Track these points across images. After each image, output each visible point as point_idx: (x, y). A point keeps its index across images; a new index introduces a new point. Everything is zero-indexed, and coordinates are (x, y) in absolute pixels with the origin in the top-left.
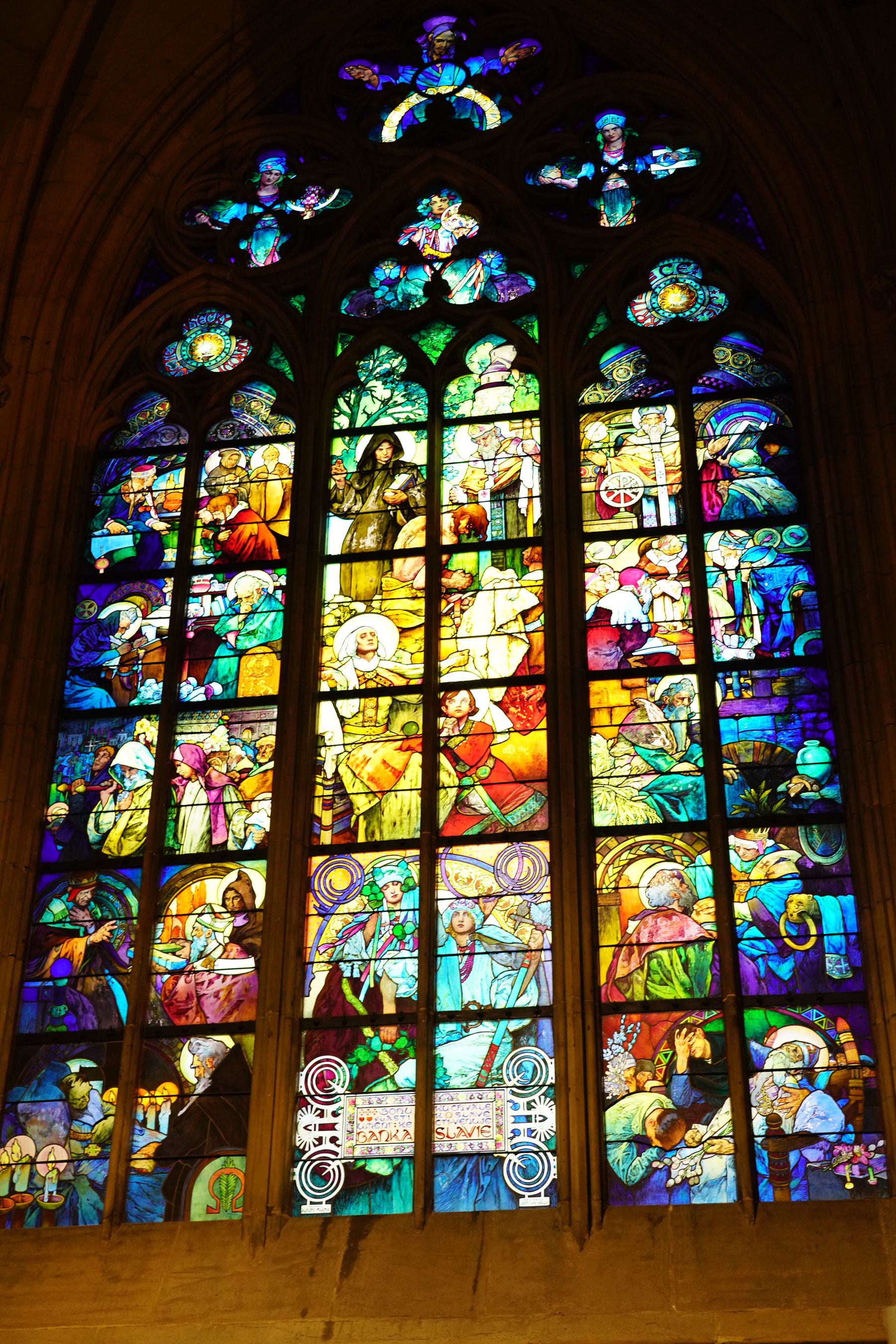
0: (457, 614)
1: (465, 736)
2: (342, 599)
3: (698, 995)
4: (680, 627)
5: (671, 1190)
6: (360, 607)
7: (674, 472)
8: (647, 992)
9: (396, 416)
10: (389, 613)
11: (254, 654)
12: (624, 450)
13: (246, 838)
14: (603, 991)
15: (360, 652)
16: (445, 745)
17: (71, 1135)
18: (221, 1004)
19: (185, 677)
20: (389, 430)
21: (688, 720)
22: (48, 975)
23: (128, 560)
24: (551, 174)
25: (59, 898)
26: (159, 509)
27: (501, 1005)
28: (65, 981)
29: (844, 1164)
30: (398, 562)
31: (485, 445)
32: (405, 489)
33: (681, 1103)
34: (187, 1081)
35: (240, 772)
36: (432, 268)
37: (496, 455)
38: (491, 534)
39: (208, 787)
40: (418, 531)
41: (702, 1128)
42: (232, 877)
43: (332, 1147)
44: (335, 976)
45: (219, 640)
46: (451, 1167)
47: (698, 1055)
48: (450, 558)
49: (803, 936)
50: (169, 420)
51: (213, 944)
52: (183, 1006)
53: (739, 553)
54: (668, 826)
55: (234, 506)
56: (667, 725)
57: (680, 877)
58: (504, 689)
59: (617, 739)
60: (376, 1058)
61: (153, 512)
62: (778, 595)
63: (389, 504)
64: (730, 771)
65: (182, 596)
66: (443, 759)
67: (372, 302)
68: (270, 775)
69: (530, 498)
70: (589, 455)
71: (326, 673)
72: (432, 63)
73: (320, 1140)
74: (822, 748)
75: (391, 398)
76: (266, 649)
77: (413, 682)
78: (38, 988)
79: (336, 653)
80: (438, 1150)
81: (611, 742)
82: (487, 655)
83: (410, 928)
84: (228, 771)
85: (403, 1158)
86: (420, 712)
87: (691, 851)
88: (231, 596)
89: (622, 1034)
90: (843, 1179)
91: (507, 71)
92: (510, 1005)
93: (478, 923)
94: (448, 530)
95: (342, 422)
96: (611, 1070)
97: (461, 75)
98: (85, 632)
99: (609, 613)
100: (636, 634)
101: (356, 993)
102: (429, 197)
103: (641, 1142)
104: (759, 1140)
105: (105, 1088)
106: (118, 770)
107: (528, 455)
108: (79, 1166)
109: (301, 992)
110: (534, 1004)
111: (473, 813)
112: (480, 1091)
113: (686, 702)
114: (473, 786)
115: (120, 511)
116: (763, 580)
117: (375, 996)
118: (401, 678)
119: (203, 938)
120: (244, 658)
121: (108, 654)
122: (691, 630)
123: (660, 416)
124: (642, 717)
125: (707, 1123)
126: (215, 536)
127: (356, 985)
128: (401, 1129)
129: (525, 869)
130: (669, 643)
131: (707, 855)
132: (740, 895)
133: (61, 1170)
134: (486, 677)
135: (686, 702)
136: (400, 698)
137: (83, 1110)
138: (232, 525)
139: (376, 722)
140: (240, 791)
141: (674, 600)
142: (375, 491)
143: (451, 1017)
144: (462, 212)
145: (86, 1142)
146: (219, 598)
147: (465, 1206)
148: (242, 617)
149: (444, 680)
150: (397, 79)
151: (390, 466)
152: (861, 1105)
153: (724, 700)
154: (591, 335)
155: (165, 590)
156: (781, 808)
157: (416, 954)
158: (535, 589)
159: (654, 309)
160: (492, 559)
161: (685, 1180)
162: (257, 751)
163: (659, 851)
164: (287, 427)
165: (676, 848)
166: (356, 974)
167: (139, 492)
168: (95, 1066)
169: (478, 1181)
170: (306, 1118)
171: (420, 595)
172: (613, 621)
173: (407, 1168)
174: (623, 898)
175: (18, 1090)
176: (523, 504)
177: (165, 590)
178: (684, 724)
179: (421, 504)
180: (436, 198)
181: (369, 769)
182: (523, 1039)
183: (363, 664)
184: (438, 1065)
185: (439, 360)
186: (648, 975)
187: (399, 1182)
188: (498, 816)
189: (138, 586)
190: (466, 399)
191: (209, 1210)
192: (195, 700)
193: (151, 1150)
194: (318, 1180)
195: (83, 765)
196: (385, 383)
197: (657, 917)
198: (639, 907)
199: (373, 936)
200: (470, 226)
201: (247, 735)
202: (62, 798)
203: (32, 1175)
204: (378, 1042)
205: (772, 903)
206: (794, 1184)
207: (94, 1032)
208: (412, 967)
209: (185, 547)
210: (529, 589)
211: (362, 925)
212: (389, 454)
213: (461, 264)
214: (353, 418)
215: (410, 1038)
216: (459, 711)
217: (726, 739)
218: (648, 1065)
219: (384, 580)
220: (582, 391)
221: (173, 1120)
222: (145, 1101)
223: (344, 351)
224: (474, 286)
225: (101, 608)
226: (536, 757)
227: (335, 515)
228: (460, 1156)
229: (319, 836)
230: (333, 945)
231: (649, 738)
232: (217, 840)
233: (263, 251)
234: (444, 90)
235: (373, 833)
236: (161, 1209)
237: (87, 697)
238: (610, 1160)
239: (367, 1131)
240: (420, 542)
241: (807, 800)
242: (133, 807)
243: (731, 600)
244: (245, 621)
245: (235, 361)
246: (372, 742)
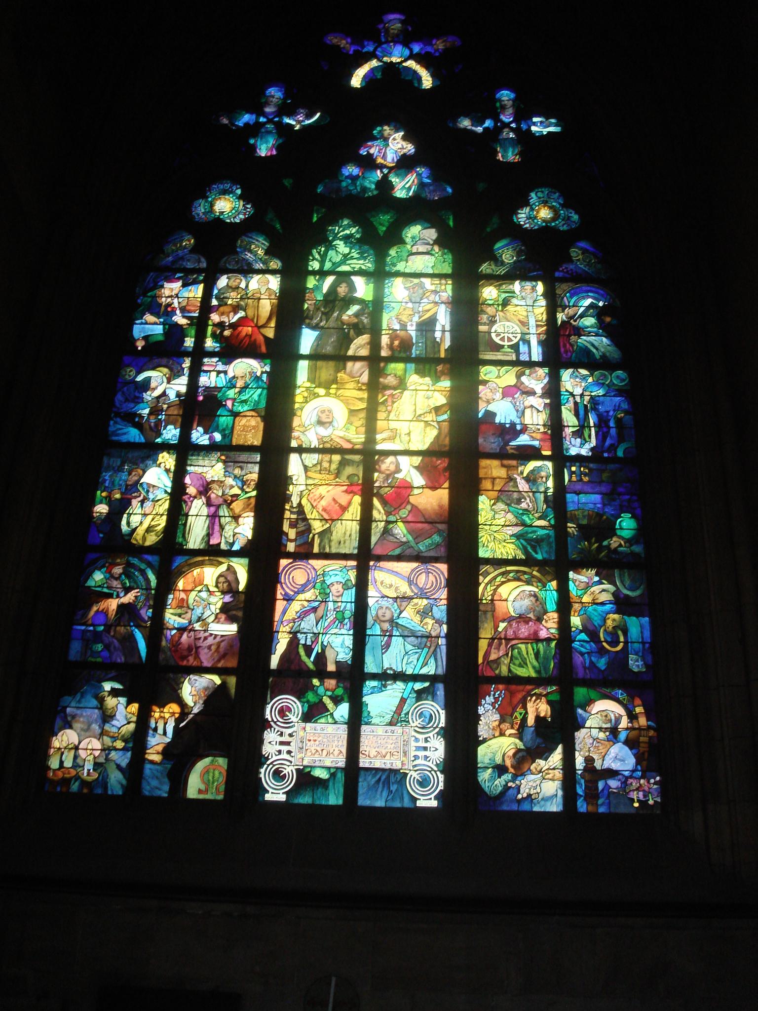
0: (390, 403)
1: (392, 487)
2: (308, 384)
3: (544, 675)
4: (542, 430)
5: (519, 802)
6: (321, 391)
7: (542, 326)
8: (510, 671)
11: (245, 416)
12: (508, 308)
13: (234, 543)
14: (480, 668)
15: (320, 423)
16: (378, 492)
17: (103, 733)
18: (212, 656)
19: (195, 425)
20: (346, 275)
21: (545, 492)
22: (90, 622)
23: (158, 343)
24: (466, 123)
25: (99, 569)
26: (183, 310)
27: (409, 672)
28: (102, 628)
29: (634, 790)
30: (349, 364)
32: (357, 315)
33: (529, 745)
34: (186, 704)
35: (232, 496)
36: (382, 172)
38: (415, 352)
39: (209, 504)
41: (541, 763)
42: (223, 568)
43: (287, 757)
44: (294, 643)
45: (220, 404)
46: (370, 778)
47: (542, 715)
49: (614, 642)
50: (194, 250)
51: (207, 613)
52: (185, 653)
53: (583, 384)
54: (528, 562)
55: (235, 313)
56: (531, 494)
57: (535, 596)
58: (420, 458)
59: (497, 499)
60: (321, 700)
61: (178, 312)
62: (608, 415)
64: (571, 527)
65: (196, 371)
66: (376, 501)
67: (339, 189)
68: (253, 501)
69: (444, 331)
70: (484, 307)
71: (295, 434)
72: (387, 42)
73: (280, 752)
74: (633, 520)
75: (349, 254)
76: (253, 413)
77: (357, 447)
78: (83, 631)
80: (361, 765)
81: (493, 502)
82: (409, 434)
83: (348, 614)
84: (223, 495)
85: (337, 768)
86: (361, 468)
87: (544, 580)
88: (231, 374)
89: (492, 697)
90: (633, 800)
91: (437, 54)
92: (416, 672)
93: (396, 615)
95: (315, 265)
96: (483, 721)
97: (407, 52)
98: (125, 389)
99: (494, 415)
100: (512, 431)
101: (309, 656)
102: (382, 126)
103: (501, 769)
104: (580, 772)
105: (129, 703)
106: (145, 486)
108: (109, 754)
109: (269, 651)
110: (432, 672)
111: (395, 540)
112: (393, 728)
113: (544, 479)
114: (396, 522)
115: (156, 309)
116: (598, 404)
117: (321, 659)
119: (201, 608)
120: (237, 418)
121: (141, 405)
122: (549, 432)
123: (534, 289)
124: (514, 487)
125: (546, 759)
126: (222, 332)
127: (309, 650)
128: (336, 749)
129: (430, 582)
130: (533, 439)
131: (554, 583)
132: (575, 611)
133: (97, 755)
135: (544, 479)
136: (347, 457)
137: (112, 717)
138: (233, 326)
139: (329, 471)
140: (231, 509)
141: (538, 411)
142: (335, 314)
143: (374, 676)
144: (404, 138)
145: (114, 739)
146: (222, 375)
147: (380, 803)
148: (237, 390)
149: (379, 447)
150: (363, 47)
152: (646, 755)
153: (570, 481)
154: (488, 230)
155: (184, 366)
156: (604, 556)
157: (351, 632)
159: (531, 218)
160: (416, 370)
161: (529, 795)
162: (244, 483)
163: (522, 577)
164: (275, 264)
165: (534, 577)
166: (309, 643)
167: (169, 297)
168: (121, 687)
169: (389, 788)
170: (270, 737)
171: (364, 388)
172: (497, 421)
173: (340, 776)
174: (497, 607)
175: (67, 699)
176: (438, 335)
177: (184, 366)
178: (542, 495)
179: (368, 327)
180: (386, 128)
181: (323, 503)
182: (424, 696)
183: (323, 432)
184: (364, 709)
185: (386, 232)
186: (511, 659)
187: (334, 784)
188: (413, 544)
189: (164, 361)
190: (401, 260)
191: (200, 791)
192: (201, 443)
193: (160, 748)
194: (277, 778)
195: (120, 480)
196: (345, 243)
197: (519, 622)
198: (506, 613)
199: (322, 617)
200: (409, 148)
201: (237, 471)
202: (104, 501)
203: (76, 757)
204: (324, 689)
205: (596, 618)
206: (600, 801)
207: (121, 664)
208: (349, 641)
209: (200, 339)
211: (314, 610)
213: (402, 171)
214: (322, 263)
215: (345, 688)
217: (570, 507)
218: (508, 719)
219: (339, 375)
220: (481, 265)
221: (176, 728)
222: (157, 715)
223: (319, 219)
224: (410, 188)
225: (139, 372)
226: (441, 507)
228: (377, 770)
229: (286, 546)
230: (294, 620)
231: (519, 502)
232: (213, 541)
233: (265, 148)
234: (395, 60)
235: (324, 548)
236: (166, 788)
237: (125, 434)
238: (480, 779)
239: (313, 749)
240: (364, 352)
241: (622, 553)
242: (154, 512)
243: (577, 414)
244: (240, 393)
245: (242, 216)
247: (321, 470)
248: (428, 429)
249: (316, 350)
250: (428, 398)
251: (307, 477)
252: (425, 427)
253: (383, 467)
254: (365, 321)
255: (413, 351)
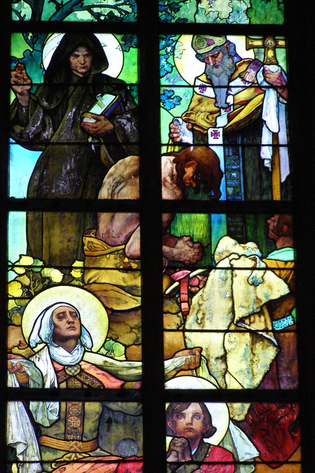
0: (184, 297)
6: (56, 275)
9: (96, 10)
10: (94, 287)
15: (57, 338)
30: (104, 217)
31: (215, 66)
32: (111, 114)
37: (230, 80)
40: (129, 177)
48: (172, 219)
58: (247, 406)
63: (89, 135)
69: (276, 146)
71: (14, 362)
79: (27, 335)
94: (169, 179)
107: (272, 86)
118: (113, 379)
134: (223, 386)
136: (113, 406)
142: (70, 114)
149: (171, 385)
151: (90, 81)
158: (284, 273)
160: (228, 227)
171: (134, 266)
176: (266, 153)
179: (133, 139)
210: (277, 272)
212: (88, 64)
216: (190, 430)
219: (87, 240)
227: (17, 142)
246: (78, 461)
247: (66, 432)
248: (259, 346)
249: (38, 189)
250: (255, 284)
251: (42, 447)
252: (253, 343)
253: (182, 423)
254: (128, 127)
255: (222, 188)
